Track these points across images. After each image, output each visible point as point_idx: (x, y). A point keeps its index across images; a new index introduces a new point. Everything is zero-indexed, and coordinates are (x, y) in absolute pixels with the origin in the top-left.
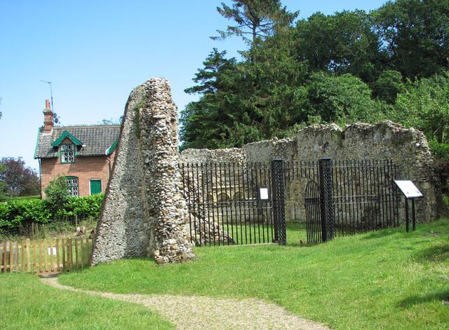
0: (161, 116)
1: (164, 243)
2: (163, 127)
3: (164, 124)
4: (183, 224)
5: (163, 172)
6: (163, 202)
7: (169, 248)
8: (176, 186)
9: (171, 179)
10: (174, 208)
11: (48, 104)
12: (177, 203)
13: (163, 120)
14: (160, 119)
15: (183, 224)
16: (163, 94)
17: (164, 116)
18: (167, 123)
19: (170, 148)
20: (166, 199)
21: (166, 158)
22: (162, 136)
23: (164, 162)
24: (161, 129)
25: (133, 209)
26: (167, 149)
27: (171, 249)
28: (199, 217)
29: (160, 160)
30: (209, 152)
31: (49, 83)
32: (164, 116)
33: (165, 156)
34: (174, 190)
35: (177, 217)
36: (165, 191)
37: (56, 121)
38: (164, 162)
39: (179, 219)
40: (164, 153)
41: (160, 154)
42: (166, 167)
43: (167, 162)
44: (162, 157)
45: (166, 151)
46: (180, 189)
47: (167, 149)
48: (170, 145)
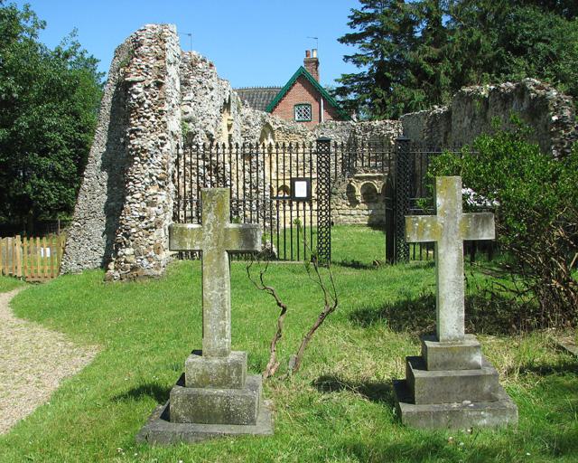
0: (136, 79)
1: (119, 253)
2: (137, 93)
3: (141, 90)
4: (152, 228)
6: (129, 198)
7: (123, 260)
8: (151, 175)
9: (145, 165)
10: (144, 205)
12: (150, 198)
13: (139, 84)
14: (135, 82)
15: (152, 228)
16: (152, 47)
18: (146, 88)
19: (148, 123)
20: (132, 193)
21: (140, 136)
22: (137, 105)
23: (135, 142)
24: (135, 96)
25: (112, 204)
27: (126, 262)
30: (353, 126)
31: (190, 35)
32: (141, 78)
33: (140, 133)
34: (147, 180)
35: (142, 218)
36: (134, 182)
38: (135, 142)
39: (146, 221)
40: (138, 130)
41: (132, 132)
42: (138, 149)
43: (141, 142)
44: (135, 135)
45: (142, 127)
47: (143, 124)
48: (148, 118)
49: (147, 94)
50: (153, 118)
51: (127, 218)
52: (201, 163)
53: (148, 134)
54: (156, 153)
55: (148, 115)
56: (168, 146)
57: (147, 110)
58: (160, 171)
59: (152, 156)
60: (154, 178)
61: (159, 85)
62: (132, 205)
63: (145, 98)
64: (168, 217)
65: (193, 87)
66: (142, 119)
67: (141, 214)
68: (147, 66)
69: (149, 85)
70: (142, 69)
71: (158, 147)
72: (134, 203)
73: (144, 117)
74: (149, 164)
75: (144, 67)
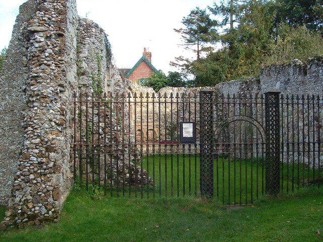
0: (38, 29)
2: (40, 42)
3: (42, 40)
8: (50, 120)
9: (44, 111)
13: (42, 34)
17: (43, 28)
18: (47, 38)
19: (48, 71)
24: (37, 45)
25: (13, 147)
26: (44, 71)
28: (117, 158)
29: (33, 85)
32: (43, 28)
40: (37, 76)
42: (38, 95)
44: (36, 80)
45: (41, 74)
46: (58, 125)
47: (44, 71)
48: (49, 65)
49: (49, 43)
50: (53, 67)
52: (90, 110)
53: (48, 81)
54: (56, 99)
55: (49, 63)
56: (67, 93)
57: (48, 59)
58: (58, 117)
59: (51, 101)
60: (53, 124)
61: (60, 35)
63: (46, 47)
64: (65, 161)
65: (87, 46)
66: (42, 67)
67: (39, 160)
68: (49, 19)
69: (51, 36)
70: (45, 20)
71: (57, 93)
72: (33, 148)
73: (45, 64)
75: (46, 19)
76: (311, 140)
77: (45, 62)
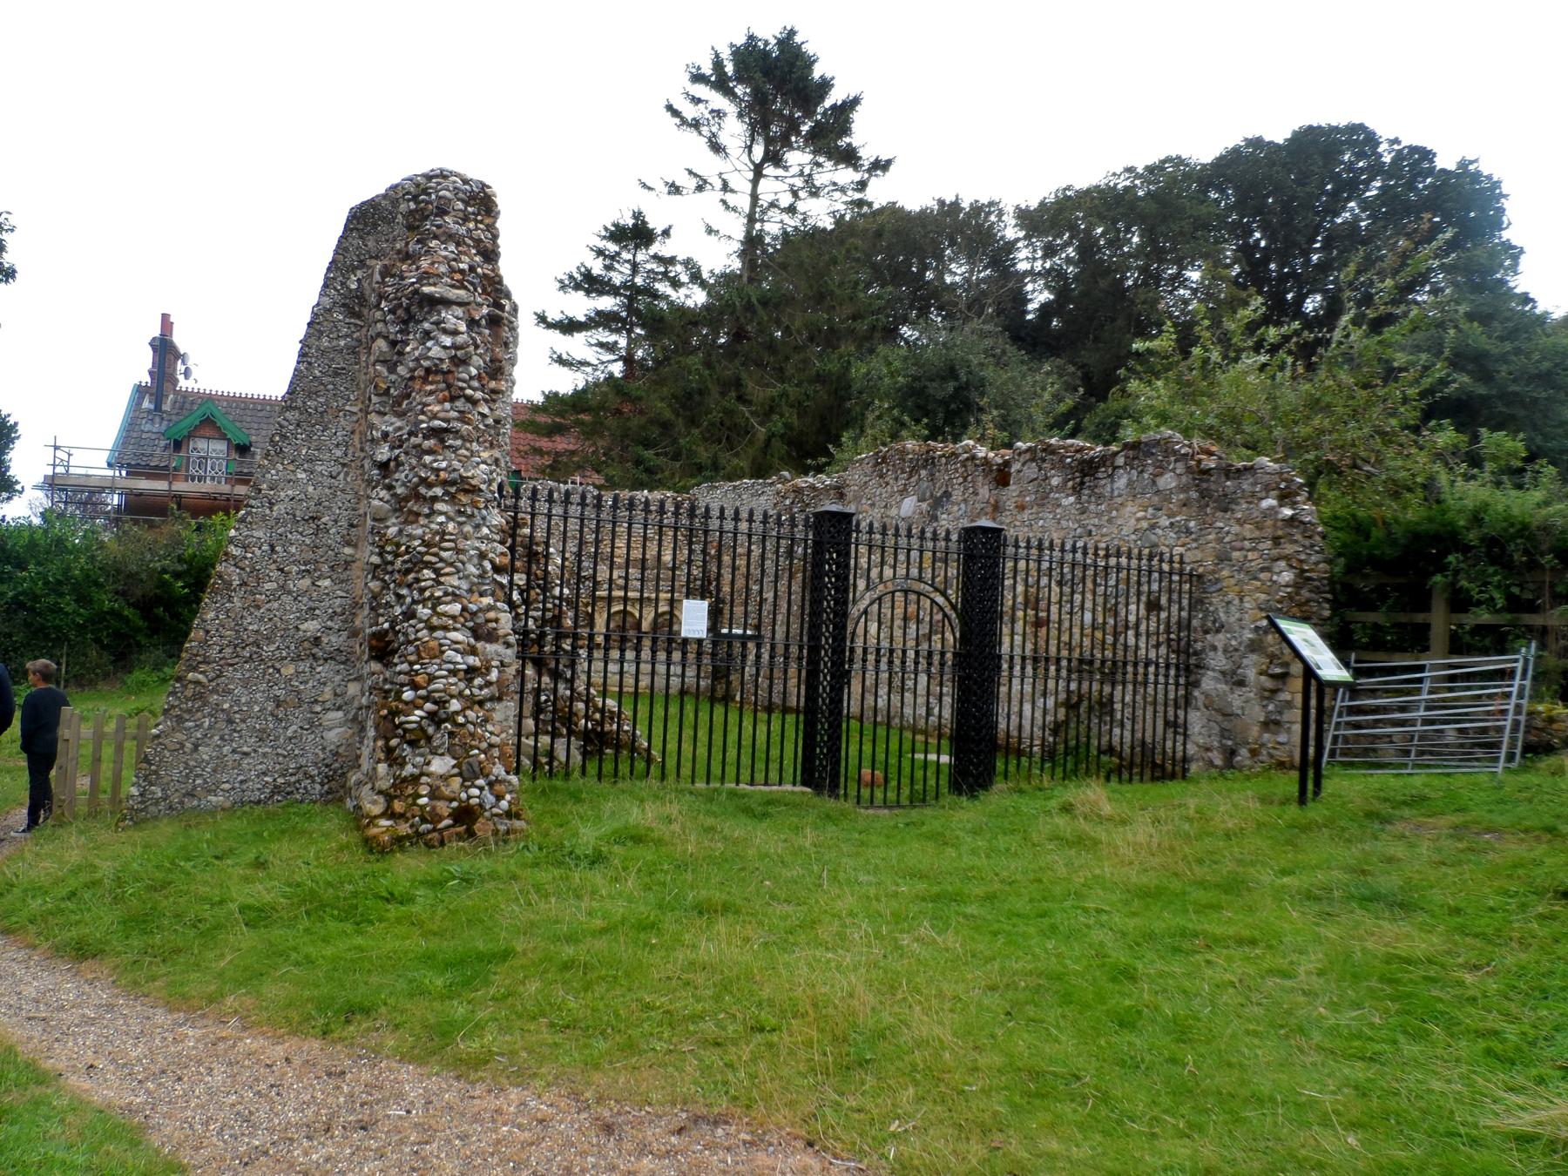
2: (455, 333)
3: (463, 327)
4: (491, 699)
5: (435, 499)
6: (423, 611)
8: (482, 556)
11: (166, 322)
12: (480, 619)
13: (459, 311)
14: (447, 303)
15: (491, 699)
18: (472, 323)
20: (437, 602)
21: (455, 449)
24: (447, 341)
28: (556, 675)
29: (430, 452)
35: (471, 672)
36: (437, 571)
37: (187, 374)
39: (478, 681)
40: (446, 430)
44: (442, 441)
45: (457, 425)
46: (497, 569)
47: (463, 418)
51: (432, 669)
60: (488, 565)
62: (439, 634)
66: (460, 404)
72: (445, 628)
73: (469, 399)
74: (477, 527)
76: (1017, 651)
77: (469, 392)
